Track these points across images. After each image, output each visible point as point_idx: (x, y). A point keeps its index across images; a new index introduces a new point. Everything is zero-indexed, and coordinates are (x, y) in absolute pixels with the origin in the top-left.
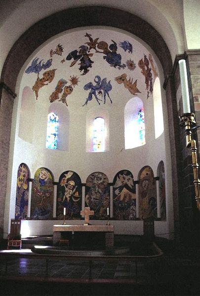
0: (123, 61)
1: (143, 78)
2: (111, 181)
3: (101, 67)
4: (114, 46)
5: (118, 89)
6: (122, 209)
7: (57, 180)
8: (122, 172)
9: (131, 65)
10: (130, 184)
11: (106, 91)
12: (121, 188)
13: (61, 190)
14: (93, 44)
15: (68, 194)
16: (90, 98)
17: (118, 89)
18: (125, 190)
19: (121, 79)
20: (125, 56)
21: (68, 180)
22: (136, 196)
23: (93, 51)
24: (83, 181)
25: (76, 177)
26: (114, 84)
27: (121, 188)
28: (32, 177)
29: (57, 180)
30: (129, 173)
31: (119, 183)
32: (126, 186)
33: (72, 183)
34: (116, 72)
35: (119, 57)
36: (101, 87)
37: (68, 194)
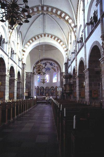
0: (53, 65)
1: (57, 69)
2: (50, 88)
3: (48, 66)
4: (52, 63)
5: (52, 70)
6: (52, 94)
7: (40, 88)
8: (52, 87)
9: (55, 66)
10: (54, 89)
11: (49, 70)
12: (52, 90)
13: (40, 90)
14: (47, 62)
15: (42, 91)
16: (46, 71)
17: (52, 70)
18: (53, 90)
19: (53, 68)
20: (54, 65)
21: (42, 88)
22: (55, 91)
23: (47, 63)
24: (45, 88)
25: (43, 88)
26: (51, 69)
27: (52, 90)
28: (36, 88)
29: (40, 88)
30: (53, 87)
31: (51, 89)
32: (53, 89)
33: (43, 89)
34: (52, 67)
35: (53, 65)
36: (48, 69)
37: (42, 91)
